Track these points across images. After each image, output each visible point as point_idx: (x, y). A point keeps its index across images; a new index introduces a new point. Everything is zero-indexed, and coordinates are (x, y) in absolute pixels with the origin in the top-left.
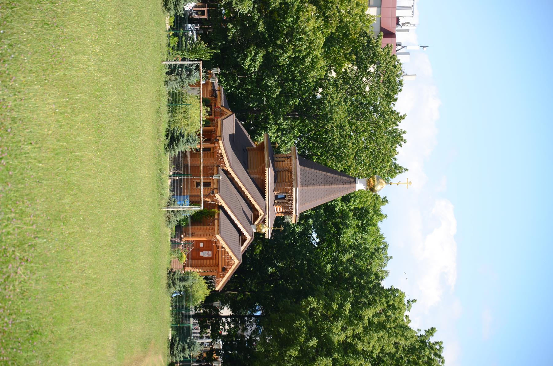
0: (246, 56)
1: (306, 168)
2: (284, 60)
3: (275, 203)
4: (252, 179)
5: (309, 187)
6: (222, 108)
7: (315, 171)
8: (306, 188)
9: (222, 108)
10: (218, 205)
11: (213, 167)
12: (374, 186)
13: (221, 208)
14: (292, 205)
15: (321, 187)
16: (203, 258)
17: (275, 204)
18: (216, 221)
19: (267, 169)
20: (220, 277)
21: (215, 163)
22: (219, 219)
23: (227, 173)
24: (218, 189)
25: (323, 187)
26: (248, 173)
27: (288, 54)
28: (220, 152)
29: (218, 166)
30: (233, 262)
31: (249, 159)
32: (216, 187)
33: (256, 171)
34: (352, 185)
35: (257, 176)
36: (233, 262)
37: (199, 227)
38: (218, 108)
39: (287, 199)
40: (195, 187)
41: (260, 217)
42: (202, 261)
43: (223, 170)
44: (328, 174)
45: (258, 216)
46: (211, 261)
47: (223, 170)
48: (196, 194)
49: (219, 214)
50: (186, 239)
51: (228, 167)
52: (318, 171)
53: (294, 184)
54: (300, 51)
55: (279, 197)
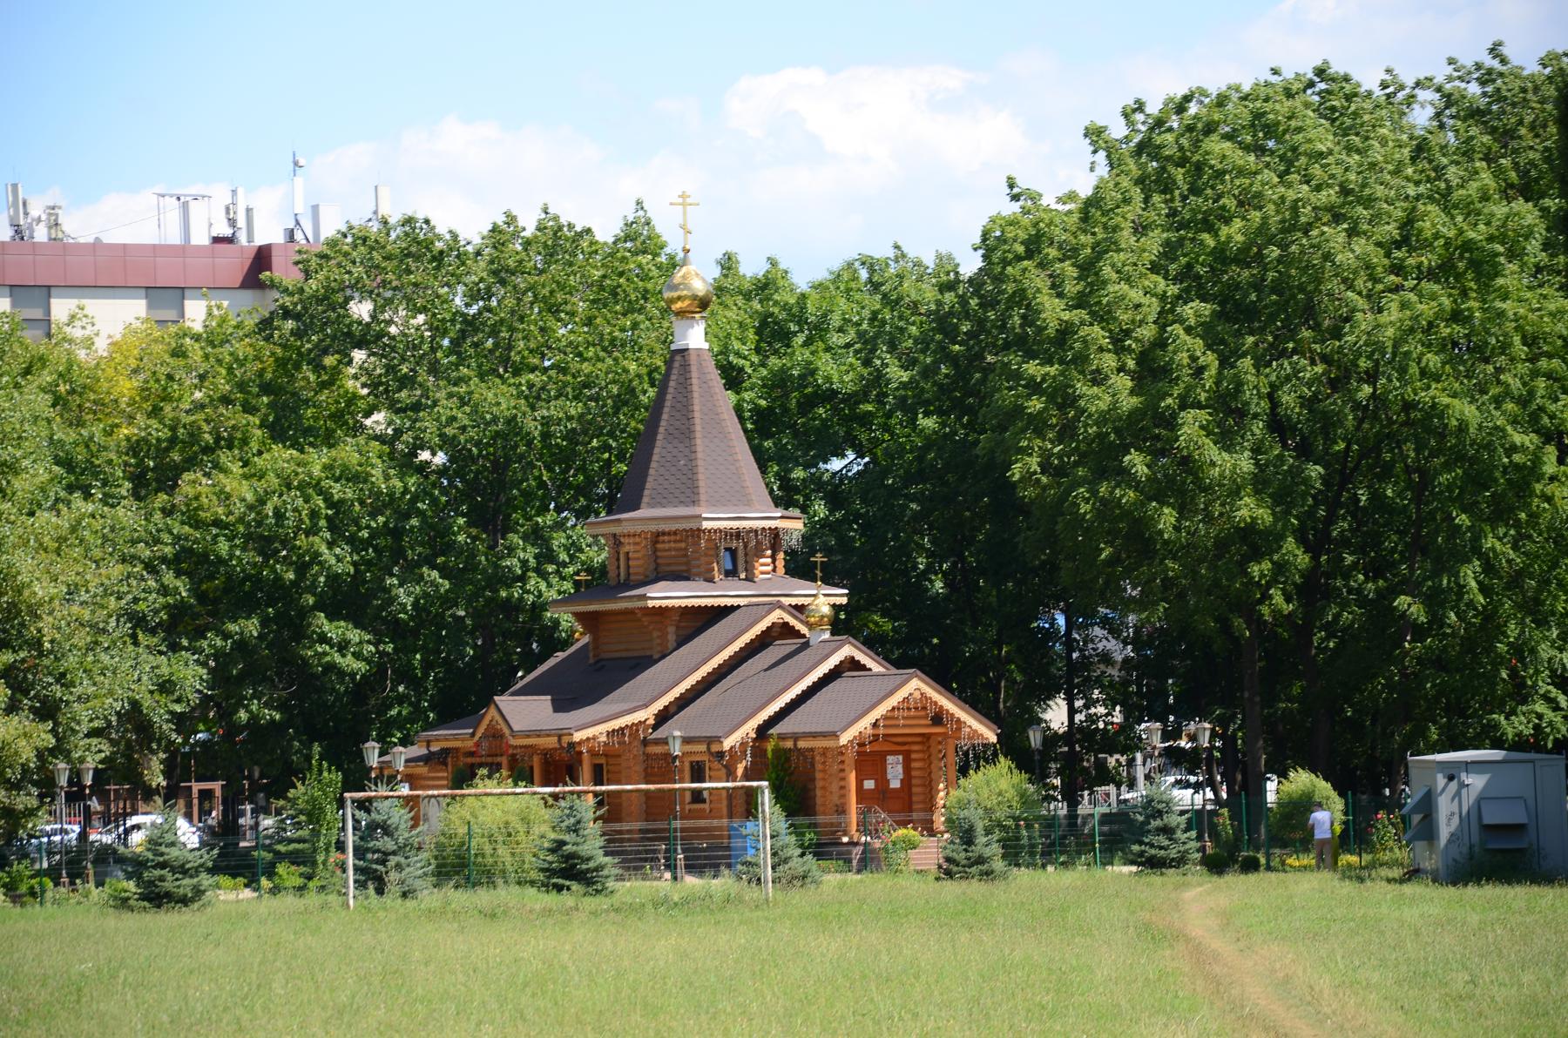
0: (331, 667)
1: (646, 492)
2: (339, 560)
4: (679, 645)
5: (701, 484)
6: (479, 735)
7: (653, 465)
8: (702, 491)
9: (479, 735)
10: (754, 740)
11: (648, 756)
12: (695, 297)
13: (762, 731)
14: (751, 530)
15: (699, 449)
16: (907, 780)
17: (750, 579)
18: (802, 744)
19: (651, 604)
20: (959, 729)
21: (637, 749)
22: (796, 737)
23: (663, 717)
25: (698, 442)
26: (663, 657)
27: (324, 549)
28: (603, 738)
29: (645, 742)
30: (917, 695)
31: (624, 654)
33: (656, 634)
34: (693, 360)
35: (671, 629)
36: (917, 695)
37: (819, 793)
38: (477, 745)
42: (914, 782)
43: (655, 727)
44: (661, 430)
45: (786, 624)
46: (914, 756)
47: (655, 727)
49: (782, 737)
50: (854, 827)
51: (647, 714)
52: (655, 458)
53: (693, 525)
54: (314, 514)
55: (729, 566)
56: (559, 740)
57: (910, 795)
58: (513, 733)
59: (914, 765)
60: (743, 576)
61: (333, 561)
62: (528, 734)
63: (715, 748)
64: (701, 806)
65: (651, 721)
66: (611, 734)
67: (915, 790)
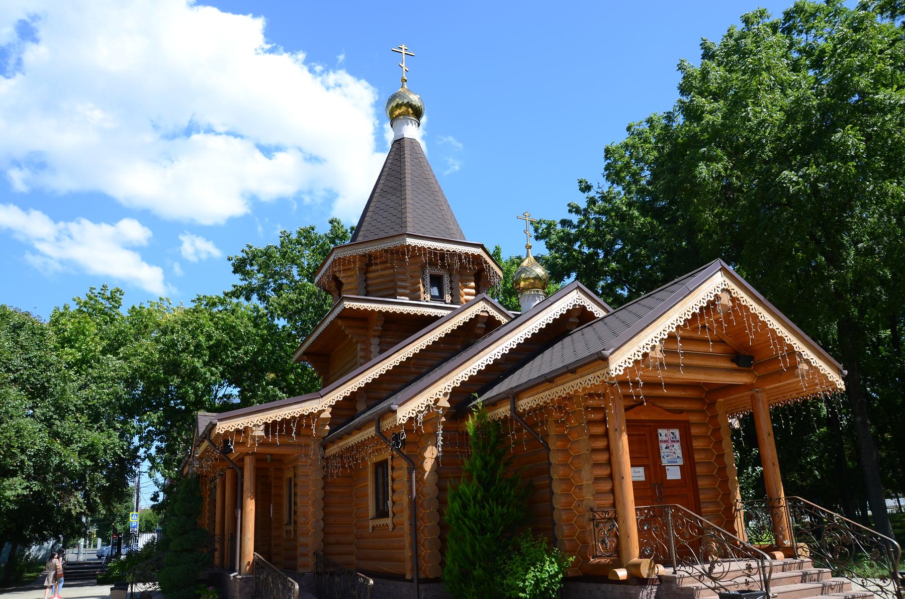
2: (212, 374)
3: (452, 303)
10: (448, 413)
11: (326, 459)
12: (409, 105)
13: (460, 397)
14: (453, 254)
16: (688, 468)
18: (526, 403)
20: (794, 367)
22: (514, 395)
33: (359, 347)
36: (725, 300)
37: (557, 488)
39: (436, 272)
42: (699, 470)
45: (491, 318)
46: (694, 431)
49: (492, 404)
50: (636, 551)
54: (198, 346)
55: (437, 294)
57: (696, 489)
59: (697, 444)
60: (448, 298)
61: (208, 375)
65: (327, 415)
66: (270, 427)
67: (702, 483)
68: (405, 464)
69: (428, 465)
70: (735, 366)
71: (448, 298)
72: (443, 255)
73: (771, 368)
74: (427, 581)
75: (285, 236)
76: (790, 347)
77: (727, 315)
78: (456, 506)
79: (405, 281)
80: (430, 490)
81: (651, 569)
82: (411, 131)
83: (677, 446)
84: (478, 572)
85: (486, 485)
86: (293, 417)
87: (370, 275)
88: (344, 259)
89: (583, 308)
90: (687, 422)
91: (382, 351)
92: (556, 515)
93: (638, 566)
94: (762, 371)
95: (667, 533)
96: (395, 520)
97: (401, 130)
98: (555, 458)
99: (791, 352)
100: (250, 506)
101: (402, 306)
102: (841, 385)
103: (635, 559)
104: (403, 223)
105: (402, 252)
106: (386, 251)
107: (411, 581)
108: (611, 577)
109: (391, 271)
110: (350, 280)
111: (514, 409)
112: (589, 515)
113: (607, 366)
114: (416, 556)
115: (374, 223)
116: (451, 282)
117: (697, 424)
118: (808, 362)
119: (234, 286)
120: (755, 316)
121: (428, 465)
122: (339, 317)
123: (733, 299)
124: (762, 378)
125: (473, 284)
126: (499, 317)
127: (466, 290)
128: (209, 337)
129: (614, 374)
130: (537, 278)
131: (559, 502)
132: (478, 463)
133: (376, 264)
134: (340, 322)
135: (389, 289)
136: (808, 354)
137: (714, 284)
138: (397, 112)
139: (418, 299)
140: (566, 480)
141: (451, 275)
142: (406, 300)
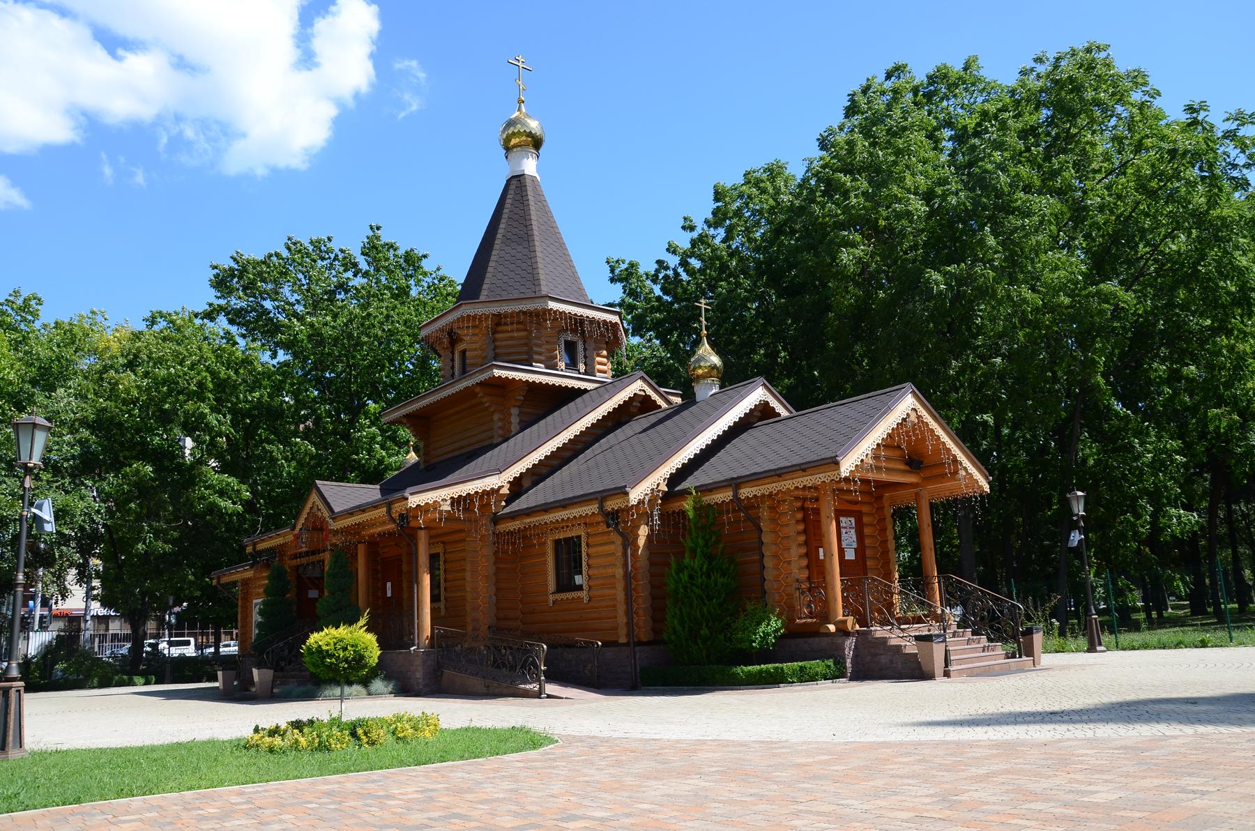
3: (586, 373)
4: (522, 429)
5: (542, 277)
6: (299, 526)
7: (491, 264)
8: (542, 283)
9: (299, 526)
11: (498, 535)
12: (530, 134)
14: (592, 321)
15: (537, 249)
16: (860, 551)
17: (590, 371)
18: (746, 492)
19: (497, 373)
20: (956, 472)
21: (485, 528)
22: (735, 483)
23: (518, 487)
24: (601, 497)
25: (537, 243)
26: (506, 440)
29: (496, 520)
31: (456, 453)
32: (591, 509)
33: (496, 417)
35: (515, 411)
36: (913, 418)
37: (769, 563)
38: (297, 537)
40: (584, 594)
41: (650, 392)
42: (868, 552)
43: (510, 499)
44: (499, 236)
45: (648, 397)
46: (866, 520)
47: (510, 499)
48: (620, 586)
50: (840, 611)
51: (500, 481)
52: (493, 258)
56: (389, 511)
58: (335, 516)
59: (867, 531)
60: (582, 367)
62: (350, 513)
63: (611, 505)
64: (579, 594)
65: (505, 491)
66: (455, 501)
68: (618, 540)
69: (642, 541)
70: (902, 467)
71: (582, 367)
72: (579, 322)
73: (936, 471)
74: (640, 643)
75: (293, 245)
76: (955, 456)
77: (914, 430)
78: (685, 577)
79: (540, 346)
80: (643, 563)
81: (854, 624)
82: (530, 166)
83: (853, 531)
84: (704, 631)
85: (709, 558)
86: (476, 493)
87: (498, 336)
88: (474, 317)
89: (767, 403)
90: (860, 512)
91: (525, 426)
92: (767, 586)
93: (845, 622)
94: (927, 473)
95: (863, 598)
96: (593, 593)
97: (520, 164)
98: (766, 538)
99: (955, 460)
100: (426, 580)
101: (538, 375)
102: (987, 488)
103: (840, 617)
104: (535, 282)
105: (542, 315)
106: (525, 313)
107: (627, 644)
108: (822, 630)
109: (524, 333)
110: (474, 338)
111: (736, 495)
112: (796, 585)
113: (838, 468)
114: (630, 624)
115: (499, 276)
116: (585, 350)
117: (869, 514)
118: (965, 469)
119: (210, 305)
120: (932, 431)
121: (642, 541)
122: (481, 384)
123: (919, 417)
124: (928, 480)
125: (605, 353)
126: (655, 397)
127: (598, 359)
128: (214, 374)
129: (843, 475)
130: (714, 367)
131: (769, 574)
132: (701, 542)
133: (506, 324)
134: (478, 389)
135: (520, 353)
136: (966, 463)
137: (906, 405)
138: (514, 141)
139: (554, 367)
140: (776, 556)
141: (585, 342)
142: (540, 367)
